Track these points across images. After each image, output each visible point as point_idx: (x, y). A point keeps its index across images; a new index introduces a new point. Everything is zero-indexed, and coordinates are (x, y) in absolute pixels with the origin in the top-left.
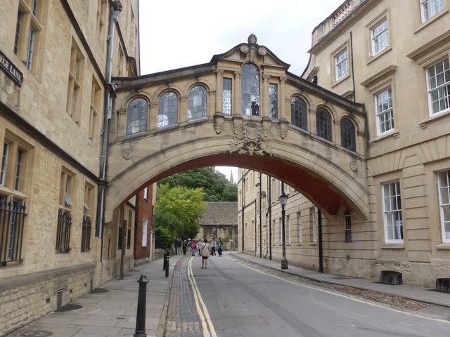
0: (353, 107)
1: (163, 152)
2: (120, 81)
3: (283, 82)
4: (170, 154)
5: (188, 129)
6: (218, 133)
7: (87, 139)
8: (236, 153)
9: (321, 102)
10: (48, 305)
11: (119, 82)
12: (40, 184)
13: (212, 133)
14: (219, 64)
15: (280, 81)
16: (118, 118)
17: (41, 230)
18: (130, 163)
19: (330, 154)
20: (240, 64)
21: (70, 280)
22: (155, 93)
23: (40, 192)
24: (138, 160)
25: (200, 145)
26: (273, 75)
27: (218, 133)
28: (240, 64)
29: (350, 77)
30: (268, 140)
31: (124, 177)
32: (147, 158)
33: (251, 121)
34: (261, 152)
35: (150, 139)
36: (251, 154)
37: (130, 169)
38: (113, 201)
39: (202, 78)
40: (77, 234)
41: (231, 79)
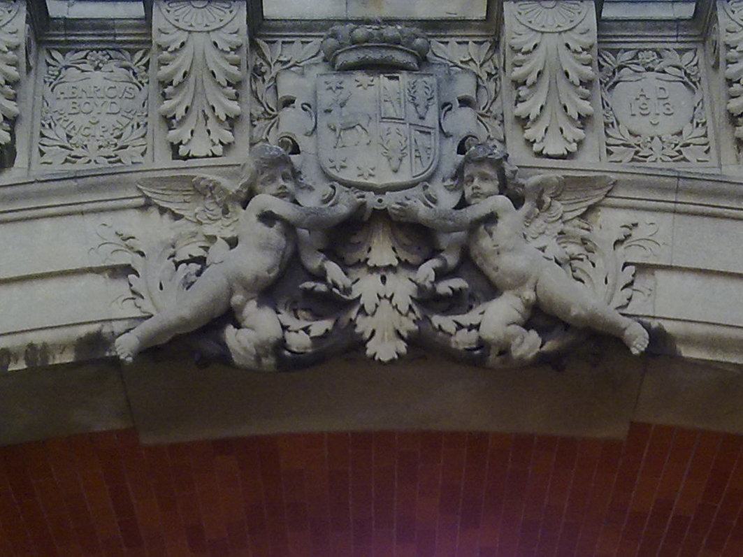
36: (384, 348)
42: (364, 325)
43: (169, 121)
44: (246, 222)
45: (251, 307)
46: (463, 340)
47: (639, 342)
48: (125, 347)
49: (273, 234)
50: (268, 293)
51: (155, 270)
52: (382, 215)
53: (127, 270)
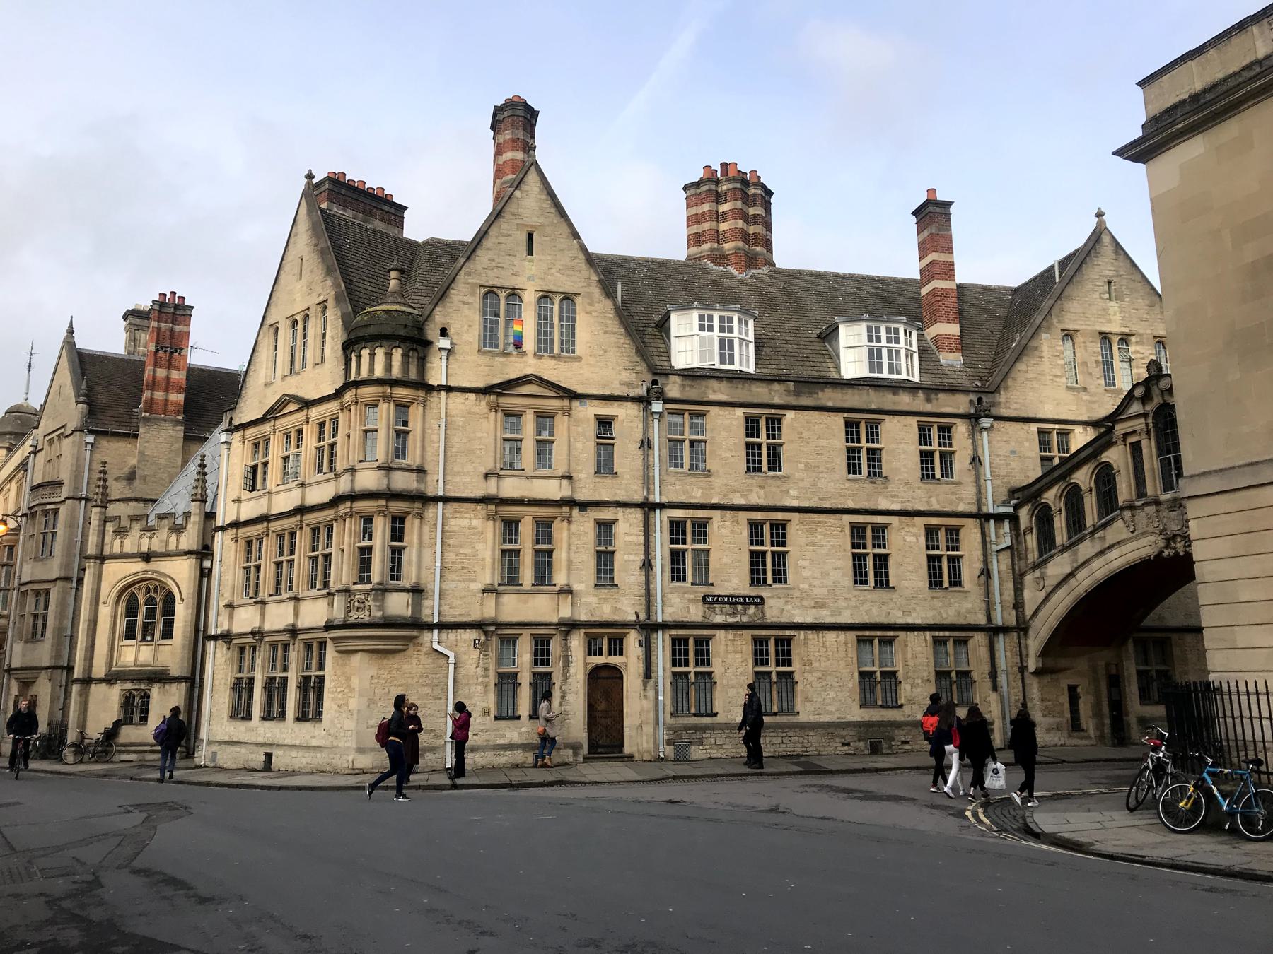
1: (1072, 575)
4: (1081, 575)
5: (1096, 536)
6: (1132, 532)
7: (927, 593)
8: (1159, 555)
10: (846, 748)
12: (812, 658)
13: (1126, 534)
14: (1118, 427)
17: (825, 691)
18: (1043, 594)
20: (1145, 415)
21: (896, 731)
22: (1056, 496)
23: (816, 665)
24: (1050, 589)
25: (1114, 554)
27: (1132, 532)
28: (1145, 415)
31: (1040, 614)
32: (1058, 586)
35: (1058, 559)
38: (1034, 644)
39: (1104, 455)
40: (919, 690)
50: (1167, 547)
51: (1154, 545)
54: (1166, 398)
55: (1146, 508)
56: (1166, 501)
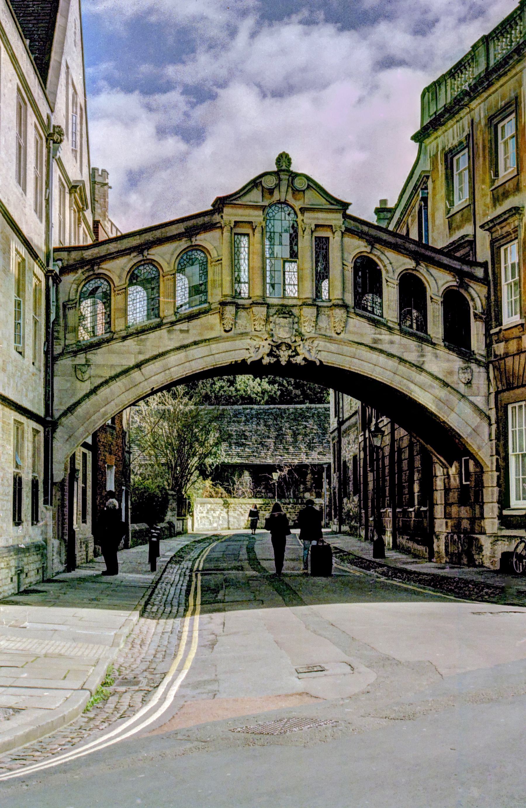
0: (466, 268)
1: (139, 366)
2: (66, 253)
3: (338, 234)
4: (148, 369)
5: (178, 327)
6: (226, 331)
9: (409, 264)
11: (64, 255)
13: (218, 331)
14: (227, 210)
15: (334, 233)
16: (65, 316)
18: (86, 387)
19: (423, 356)
20: (263, 208)
24: (99, 381)
26: (321, 222)
27: (226, 331)
28: (263, 208)
29: (469, 205)
30: (313, 339)
31: (80, 410)
33: (283, 305)
34: (299, 360)
35: (116, 345)
36: (283, 363)
37: (87, 396)
39: (198, 237)
41: (248, 235)
42: (281, 359)
43: (255, 325)
44: (266, 343)
45: (266, 357)
46: (294, 362)
47: (318, 363)
48: (249, 362)
49: (270, 347)
50: (268, 355)
51: (252, 350)
52: (285, 343)
53: (248, 349)
54: (287, 199)
55: (255, 309)
56: (274, 306)
